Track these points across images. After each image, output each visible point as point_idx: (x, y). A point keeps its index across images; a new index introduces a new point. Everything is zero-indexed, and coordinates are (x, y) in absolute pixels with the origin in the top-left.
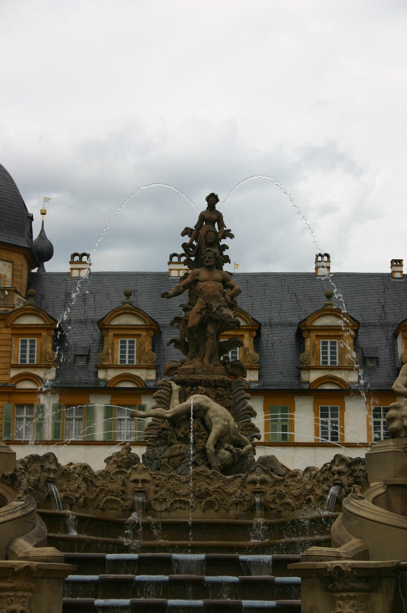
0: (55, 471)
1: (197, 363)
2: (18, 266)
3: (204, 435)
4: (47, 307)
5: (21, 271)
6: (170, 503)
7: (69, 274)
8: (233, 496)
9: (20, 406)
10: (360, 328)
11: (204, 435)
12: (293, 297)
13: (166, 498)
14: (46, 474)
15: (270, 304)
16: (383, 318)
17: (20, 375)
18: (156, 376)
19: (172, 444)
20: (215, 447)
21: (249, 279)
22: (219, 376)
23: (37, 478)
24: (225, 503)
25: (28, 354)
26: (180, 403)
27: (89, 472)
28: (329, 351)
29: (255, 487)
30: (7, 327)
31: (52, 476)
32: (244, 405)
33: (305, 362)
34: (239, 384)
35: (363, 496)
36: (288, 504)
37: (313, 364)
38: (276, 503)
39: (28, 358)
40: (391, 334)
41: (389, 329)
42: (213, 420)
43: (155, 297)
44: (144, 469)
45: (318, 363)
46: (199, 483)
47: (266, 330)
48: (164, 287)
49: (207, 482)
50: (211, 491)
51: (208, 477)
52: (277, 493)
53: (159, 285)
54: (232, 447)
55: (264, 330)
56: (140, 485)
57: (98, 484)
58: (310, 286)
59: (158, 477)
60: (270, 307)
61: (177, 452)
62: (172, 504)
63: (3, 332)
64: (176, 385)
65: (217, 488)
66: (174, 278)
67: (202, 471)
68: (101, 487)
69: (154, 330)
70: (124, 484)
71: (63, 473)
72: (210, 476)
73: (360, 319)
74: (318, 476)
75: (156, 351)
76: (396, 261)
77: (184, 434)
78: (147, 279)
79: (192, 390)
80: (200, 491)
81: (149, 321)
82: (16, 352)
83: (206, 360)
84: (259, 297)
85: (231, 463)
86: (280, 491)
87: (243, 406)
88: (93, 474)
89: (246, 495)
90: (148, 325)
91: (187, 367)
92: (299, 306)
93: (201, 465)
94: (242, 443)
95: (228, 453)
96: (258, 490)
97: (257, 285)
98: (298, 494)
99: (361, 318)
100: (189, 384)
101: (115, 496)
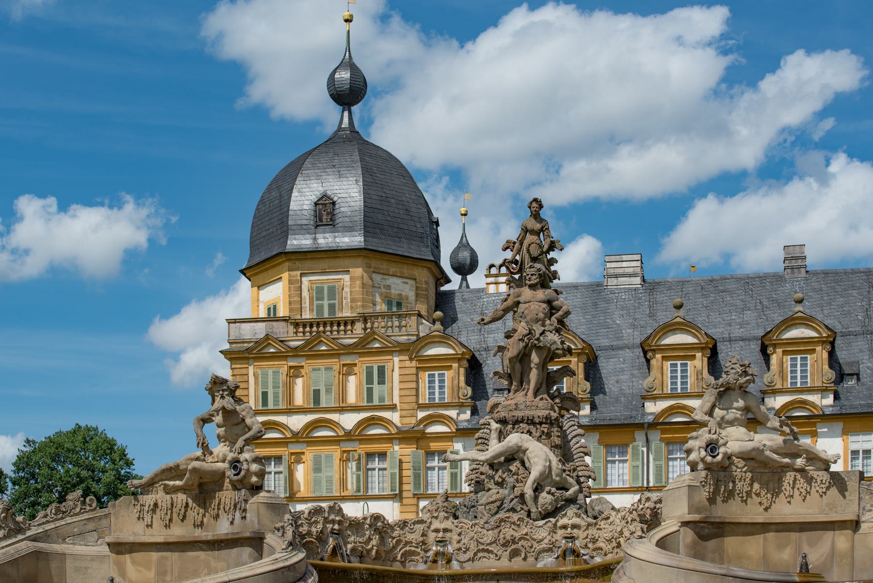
1: (520, 397)
2: (422, 284)
3: (524, 478)
4: (460, 333)
7: (482, 290)
10: (837, 338)
11: (524, 478)
12: (758, 304)
13: (469, 548)
14: (330, 526)
15: (730, 314)
17: (429, 416)
18: (591, 411)
19: (489, 489)
20: (536, 490)
21: (704, 284)
23: (319, 530)
24: (533, 550)
25: (437, 390)
26: (500, 442)
27: (383, 522)
29: (566, 532)
30: (411, 359)
31: (336, 527)
32: (578, 443)
34: (571, 419)
35: (643, 535)
36: (601, 549)
38: (589, 548)
39: (437, 395)
42: (532, 461)
43: (590, 313)
44: (445, 517)
48: (600, 300)
49: (513, 529)
50: (517, 539)
51: (514, 523)
52: (589, 537)
53: (594, 298)
54: (553, 490)
55: (721, 347)
56: (441, 534)
57: (394, 535)
59: (460, 525)
60: (729, 318)
61: (494, 498)
62: (475, 554)
64: (496, 424)
66: (612, 287)
67: (508, 517)
68: (398, 538)
70: (423, 535)
71: (350, 524)
72: (516, 522)
73: (838, 328)
74: (627, 516)
75: (591, 380)
77: (502, 478)
79: (513, 428)
81: (580, 343)
82: (423, 389)
85: (554, 508)
86: (593, 535)
87: (576, 444)
88: (388, 524)
89: (557, 540)
91: (509, 402)
92: (765, 315)
93: (520, 511)
94: (567, 486)
95: (550, 497)
96: (569, 535)
98: (611, 537)
99: (840, 326)
100: (510, 422)
101: (415, 547)
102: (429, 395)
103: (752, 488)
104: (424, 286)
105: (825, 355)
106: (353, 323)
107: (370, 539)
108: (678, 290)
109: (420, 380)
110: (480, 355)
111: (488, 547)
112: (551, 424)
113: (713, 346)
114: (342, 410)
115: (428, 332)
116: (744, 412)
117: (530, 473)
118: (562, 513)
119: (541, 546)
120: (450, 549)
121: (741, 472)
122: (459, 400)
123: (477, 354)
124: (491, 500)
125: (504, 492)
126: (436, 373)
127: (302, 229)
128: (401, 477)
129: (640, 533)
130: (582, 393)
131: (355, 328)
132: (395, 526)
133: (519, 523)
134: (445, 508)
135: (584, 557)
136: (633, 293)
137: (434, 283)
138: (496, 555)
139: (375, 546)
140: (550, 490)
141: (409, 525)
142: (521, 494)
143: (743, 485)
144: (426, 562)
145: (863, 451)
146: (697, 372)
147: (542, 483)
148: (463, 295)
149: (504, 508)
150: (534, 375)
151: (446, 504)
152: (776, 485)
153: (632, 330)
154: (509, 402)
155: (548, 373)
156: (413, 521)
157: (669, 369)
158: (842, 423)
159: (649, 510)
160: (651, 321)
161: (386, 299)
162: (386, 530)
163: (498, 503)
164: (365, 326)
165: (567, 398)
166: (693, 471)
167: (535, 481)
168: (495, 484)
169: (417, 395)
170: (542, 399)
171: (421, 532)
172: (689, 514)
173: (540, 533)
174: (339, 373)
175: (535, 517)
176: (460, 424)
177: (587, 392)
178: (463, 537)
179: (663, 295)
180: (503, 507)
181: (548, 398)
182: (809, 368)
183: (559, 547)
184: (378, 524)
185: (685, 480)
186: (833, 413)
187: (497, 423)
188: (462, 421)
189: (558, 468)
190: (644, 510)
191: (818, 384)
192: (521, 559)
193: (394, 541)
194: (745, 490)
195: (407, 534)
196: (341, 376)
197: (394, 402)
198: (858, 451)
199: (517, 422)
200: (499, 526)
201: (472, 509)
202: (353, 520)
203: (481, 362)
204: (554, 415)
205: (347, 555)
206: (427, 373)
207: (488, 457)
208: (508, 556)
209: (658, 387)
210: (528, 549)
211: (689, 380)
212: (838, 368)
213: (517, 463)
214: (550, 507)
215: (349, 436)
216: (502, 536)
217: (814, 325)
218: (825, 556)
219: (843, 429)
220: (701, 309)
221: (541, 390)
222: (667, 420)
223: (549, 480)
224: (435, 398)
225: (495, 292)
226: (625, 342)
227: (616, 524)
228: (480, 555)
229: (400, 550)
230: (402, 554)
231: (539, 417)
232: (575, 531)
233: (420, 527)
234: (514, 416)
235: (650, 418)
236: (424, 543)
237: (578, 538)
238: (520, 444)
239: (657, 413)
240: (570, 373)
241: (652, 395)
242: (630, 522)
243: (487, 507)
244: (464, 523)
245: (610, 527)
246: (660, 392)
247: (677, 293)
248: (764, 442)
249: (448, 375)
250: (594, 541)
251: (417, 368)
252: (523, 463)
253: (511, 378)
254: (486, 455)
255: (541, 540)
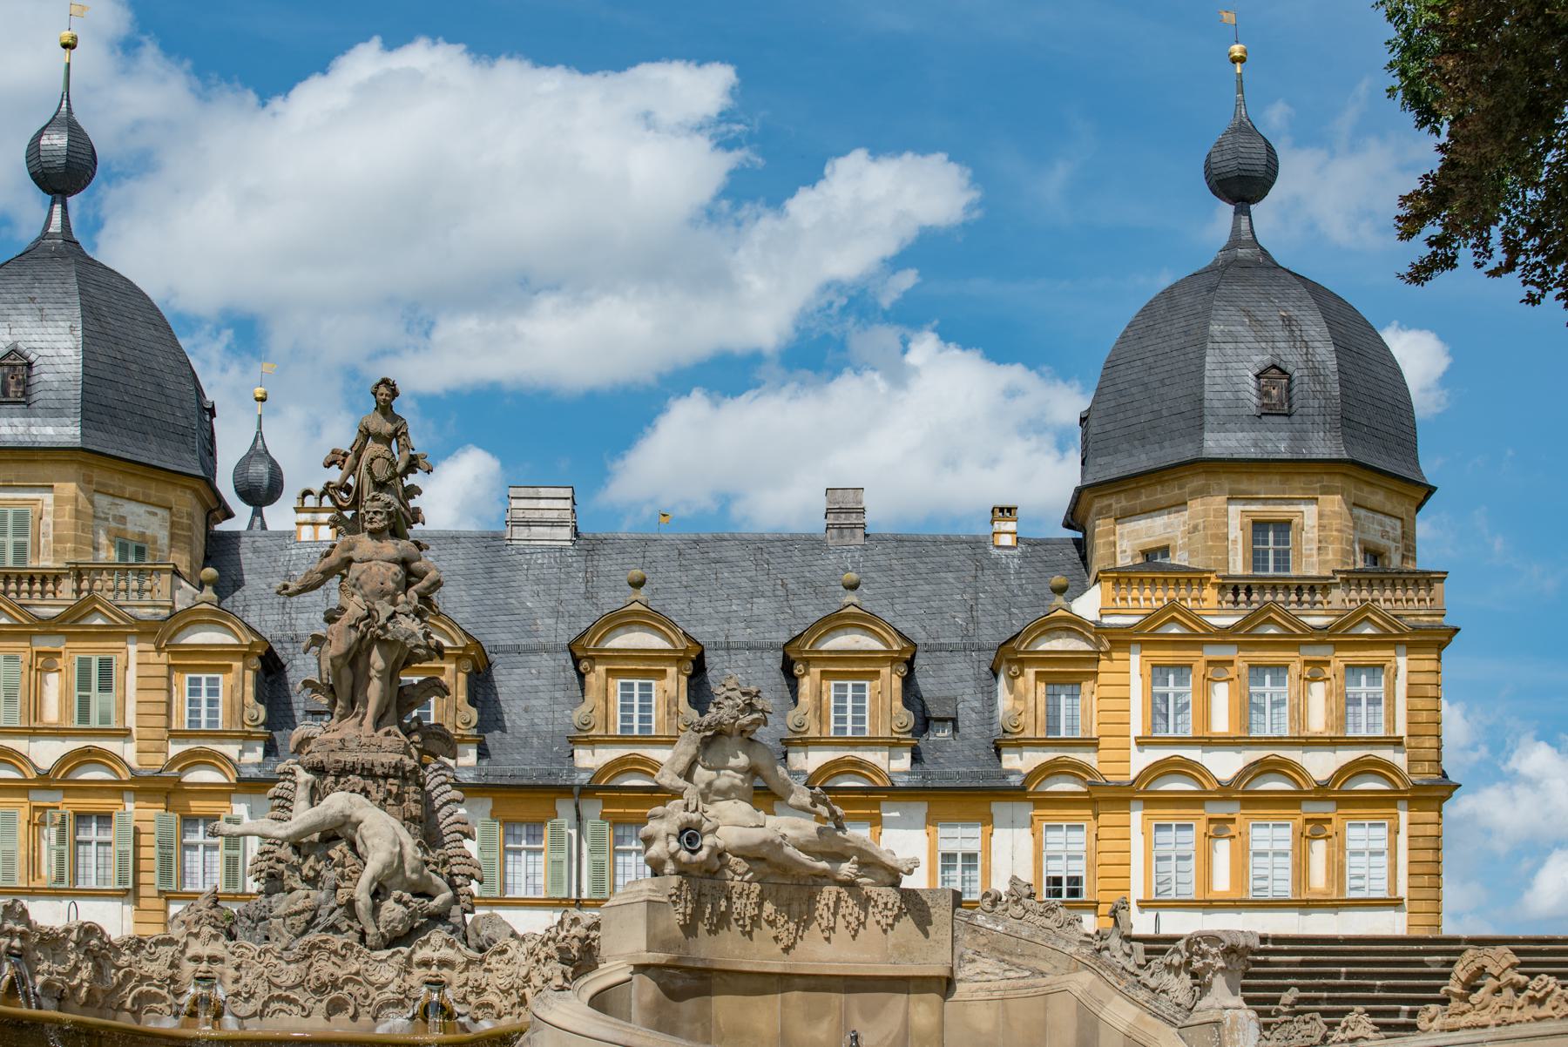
0: (23, 936)
1: (349, 728)
3: (354, 872)
4: (247, 608)
5: (190, 529)
6: (262, 1000)
7: (290, 534)
8: (385, 990)
9: (189, 821)
10: (918, 654)
11: (354, 872)
12: (780, 587)
13: (255, 993)
15: (728, 602)
16: (971, 631)
19: (292, 890)
20: (375, 895)
21: (683, 546)
22: (391, 755)
24: (368, 1001)
25: (204, 708)
26: (312, 805)
27: (100, 939)
28: (849, 704)
29: (429, 973)
30: (159, 650)
31: (17, 943)
32: (451, 814)
33: (799, 729)
35: (566, 985)
36: (492, 1006)
37: (813, 733)
38: (470, 1004)
39: (204, 717)
40: (987, 669)
41: (982, 657)
42: (369, 843)
44: (212, 935)
45: (825, 730)
46: (317, 964)
47: (717, 660)
49: (334, 963)
50: (341, 980)
51: (335, 953)
52: (470, 983)
53: (488, 560)
54: (407, 896)
55: (711, 659)
56: (204, 966)
57: (120, 963)
58: (815, 563)
60: (727, 609)
62: (266, 1004)
63: (151, 661)
65: (354, 974)
66: (520, 542)
67: (325, 942)
68: (127, 969)
69: (472, 658)
70: (173, 965)
71: (41, 939)
73: (920, 637)
74: (537, 950)
75: (479, 703)
76: (1002, 510)
77: (315, 870)
78: (464, 545)
79: (337, 783)
80: (318, 979)
82: (179, 705)
83: (369, 721)
84: (704, 588)
85: (408, 929)
86: (476, 981)
87: (448, 817)
88: (110, 943)
89: (412, 987)
90: (460, 648)
91: (329, 736)
92: (790, 607)
93: (347, 931)
94: (432, 891)
95: (401, 908)
96: (434, 979)
97: (702, 561)
98: (508, 986)
102: (190, 716)
103: (761, 910)
104: (185, 521)
105: (897, 683)
106: (57, 579)
107: (76, 969)
108: (637, 555)
109: (175, 688)
110: (283, 648)
111: (288, 993)
112: (405, 779)
113: (697, 656)
114: (33, 733)
115: (190, 602)
116: (749, 775)
117: (365, 864)
118: (422, 938)
119: (383, 996)
120: (221, 993)
121: (742, 881)
122: (243, 727)
123: (276, 647)
124: (296, 908)
125: (319, 895)
126: (204, 677)
127: (1232, 419)
128: (137, 859)
129: (560, 981)
130: (463, 727)
131: (60, 588)
132: (122, 946)
133: (344, 952)
134: (213, 920)
135: (461, 1020)
136: (557, 554)
137: (204, 516)
138: (303, 1009)
139: (85, 980)
140: (401, 896)
141: (147, 947)
142: (348, 900)
143: (746, 904)
144: (176, 1015)
145: (963, 855)
146: (669, 702)
147: (387, 884)
148: (254, 542)
149: (319, 924)
150: (375, 690)
151: (214, 912)
152: (804, 907)
153: (554, 620)
154: (329, 736)
155: (401, 689)
156: (154, 940)
157: (619, 692)
158: (926, 804)
159: (576, 940)
160: (588, 606)
161: (118, 540)
162: (104, 954)
163: (307, 916)
164: (79, 586)
165: (433, 733)
166: (656, 875)
167: (374, 879)
168: (303, 881)
169: (168, 715)
170: (388, 734)
171: (169, 959)
172: (648, 951)
173: (382, 973)
174: (30, 666)
175: (373, 944)
176: (244, 770)
177: (473, 724)
178: (243, 972)
179: (610, 562)
180: (316, 922)
181: (400, 733)
182: (867, 704)
183: (416, 1000)
184: (92, 942)
185: (641, 891)
186: (910, 785)
187: (307, 771)
188: (247, 766)
189: (415, 858)
190: (567, 940)
191: (884, 732)
192: (347, 1017)
193: (121, 974)
194: (748, 914)
195: (144, 962)
196: (33, 673)
197: (127, 725)
198: (955, 855)
199: (343, 772)
200: (309, 957)
201: (261, 924)
202: (47, 933)
203: (284, 661)
204: (410, 763)
205: (34, 993)
206: (187, 676)
207: (290, 831)
208: (324, 1010)
209: (599, 722)
210: (360, 1000)
211: (653, 714)
212: (919, 708)
213: (342, 846)
214: (400, 926)
215: (45, 781)
216: (313, 975)
217: (877, 629)
218: (891, 1038)
219: (928, 815)
220: (678, 590)
221: (386, 718)
222: (614, 783)
223: (399, 879)
224: (200, 722)
225: (312, 539)
226: (542, 640)
227: (519, 962)
228: (275, 1006)
229: (131, 990)
230: (135, 999)
231: (383, 765)
232: (445, 971)
233: (166, 952)
234: (338, 762)
235: (584, 778)
236: (173, 980)
237: (450, 984)
238: (347, 812)
239: (596, 770)
240: (439, 690)
241: (587, 737)
242: (543, 961)
243: (288, 922)
244: (246, 948)
245: (508, 967)
246: (603, 733)
247: (635, 560)
248: (783, 831)
249: (224, 680)
250: (479, 990)
251: (170, 666)
252: (353, 845)
253: (334, 693)
254: (287, 828)
255: (384, 986)
